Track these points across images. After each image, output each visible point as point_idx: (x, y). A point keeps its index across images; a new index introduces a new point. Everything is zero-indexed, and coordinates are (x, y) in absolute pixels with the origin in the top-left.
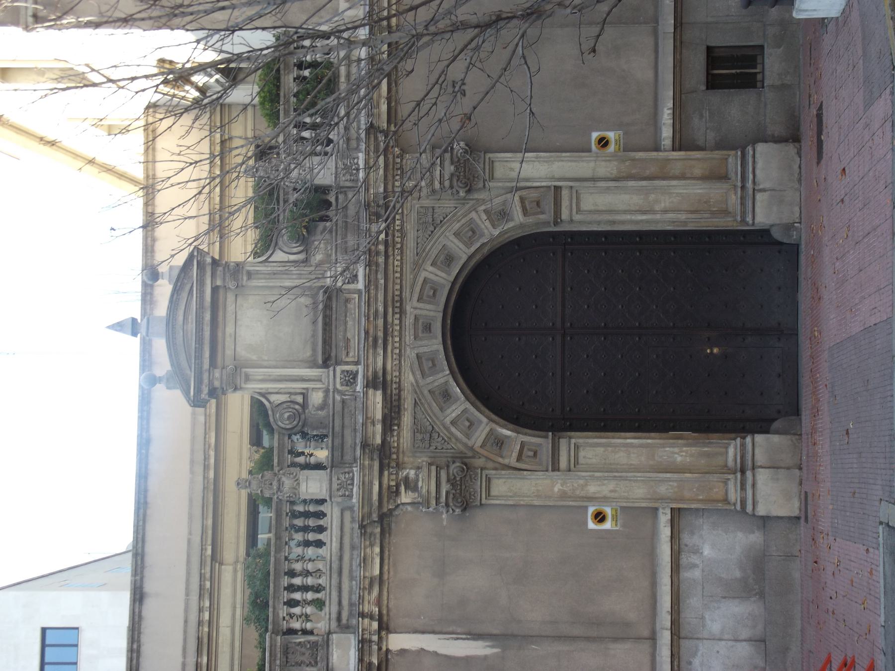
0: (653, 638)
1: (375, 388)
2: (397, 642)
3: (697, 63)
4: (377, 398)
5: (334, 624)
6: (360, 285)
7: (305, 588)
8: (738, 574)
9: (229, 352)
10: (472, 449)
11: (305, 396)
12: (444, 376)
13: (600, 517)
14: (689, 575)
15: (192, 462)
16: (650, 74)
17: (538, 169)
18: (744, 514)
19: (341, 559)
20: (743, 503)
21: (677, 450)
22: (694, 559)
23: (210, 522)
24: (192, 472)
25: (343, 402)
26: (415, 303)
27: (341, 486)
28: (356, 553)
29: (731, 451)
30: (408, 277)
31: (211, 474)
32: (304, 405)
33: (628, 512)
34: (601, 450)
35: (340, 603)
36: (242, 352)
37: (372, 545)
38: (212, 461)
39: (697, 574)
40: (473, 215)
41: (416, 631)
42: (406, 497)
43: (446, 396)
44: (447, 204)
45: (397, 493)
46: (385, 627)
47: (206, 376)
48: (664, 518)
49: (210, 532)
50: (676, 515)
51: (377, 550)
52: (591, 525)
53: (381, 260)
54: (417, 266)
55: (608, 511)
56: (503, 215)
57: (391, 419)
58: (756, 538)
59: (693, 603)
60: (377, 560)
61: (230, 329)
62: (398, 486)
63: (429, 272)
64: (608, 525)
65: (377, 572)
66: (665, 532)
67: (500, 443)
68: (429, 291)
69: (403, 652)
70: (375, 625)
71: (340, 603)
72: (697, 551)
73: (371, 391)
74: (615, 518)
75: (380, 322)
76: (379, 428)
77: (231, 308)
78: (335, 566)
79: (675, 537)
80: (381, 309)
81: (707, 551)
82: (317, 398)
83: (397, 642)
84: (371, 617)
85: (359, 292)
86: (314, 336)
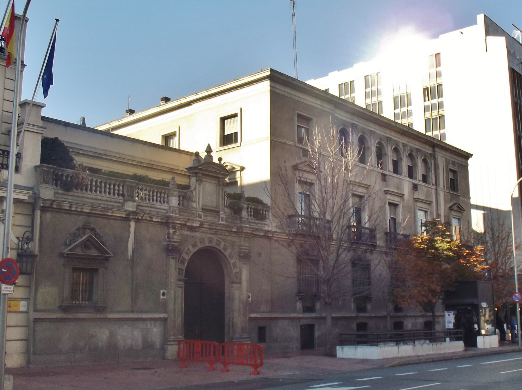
0: (133, 312)
1: (200, 224)
2: (132, 224)
3: (262, 324)
4: (197, 224)
5: (138, 204)
6: (221, 222)
7: (110, 189)
8: (149, 340)
9: (206, 180)
10: (182, 253)
11: (194, 201)
12: (200, 246)
13: (164, 294)
14: (149, 325)
15: (106, 151)
16: (262, 310)
17: (245, 276)
18: (165, 341)
19: (155, 208)
20: (170, 341)
21: (180, 321)
22: (153, 325)
23: (90, 154)
24: (103, 150)
25: (194, 214)
26: (216, 238)
27: (175, 210)
28: (156, 213)
29: (181, 337)
30: (221, 237)
31: (104, 157)
32: (192, 201)
33: (165, 304)
34: (181, 295)
35: (143, 206)
36: (204, 183)
37: (161, 219)
38: (108, 158)
39: (149, 326)
40: (235, 258)
41: (135, 231)
42: (171, 231)
43: (194, 246)
44: (237, 250)
45: (173, 228)
46: (137, 221)
47: (201, 172)
48: (162, 316)
49: (87, 153)
50: (165, 320)
51: (159, 220)
52: (162, 291)
53: (228, 229)
54: (224, 240)
55: (165, 297)
56: (235, 266)
57: (192, 229)
58: (158, 345)
59: (141, 325)
60: (156, 220)
61: (209, 180)
62: (175, 229)
63: (223, 243)
64: (161, 297)
65: (154, 220)
66: (157, 316)
67: (183, 262)
68: (218, 243)
69: (129, 226)
70: (140, 218)
71: (143, 206)
72: (155, 326)
73: (199, 223)
74: (164, 299)
75: (214, 227)
76: (190, 224)
77: (214, 182)
78: (153, 206)
79: (160, 319)
80: (218, 228)
81: (155, 330)
82: (194, 205)
83: (132, 224)
84: (142, 217)
85: (219, 221)
86: (207, 206)
